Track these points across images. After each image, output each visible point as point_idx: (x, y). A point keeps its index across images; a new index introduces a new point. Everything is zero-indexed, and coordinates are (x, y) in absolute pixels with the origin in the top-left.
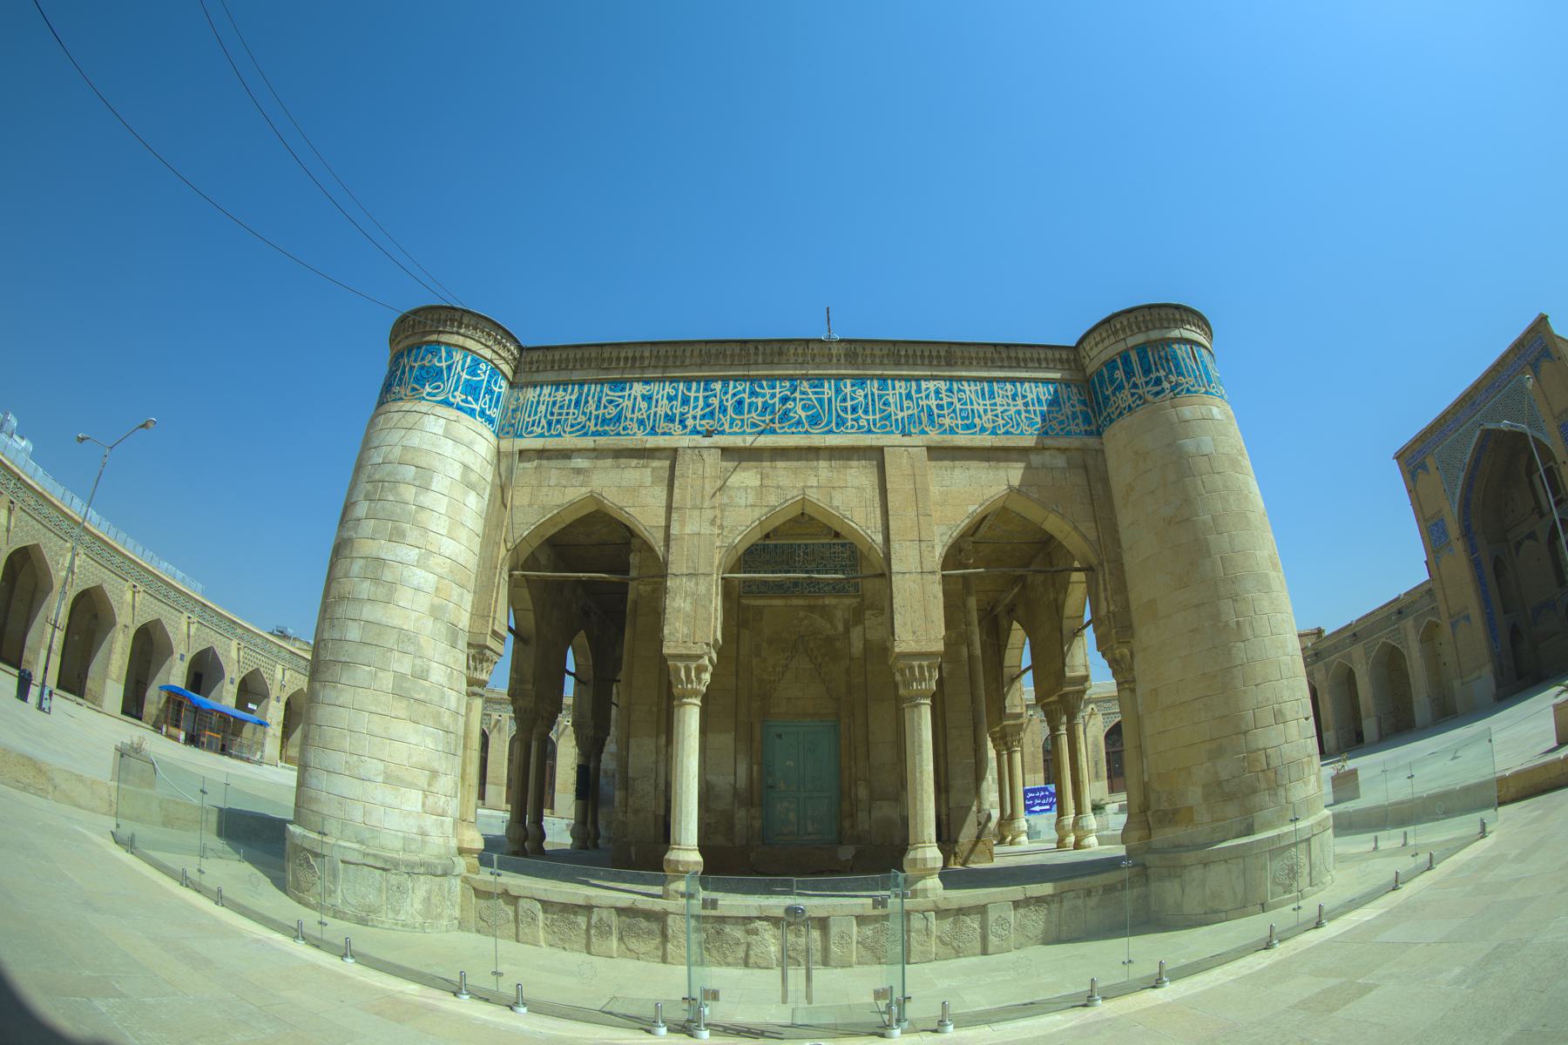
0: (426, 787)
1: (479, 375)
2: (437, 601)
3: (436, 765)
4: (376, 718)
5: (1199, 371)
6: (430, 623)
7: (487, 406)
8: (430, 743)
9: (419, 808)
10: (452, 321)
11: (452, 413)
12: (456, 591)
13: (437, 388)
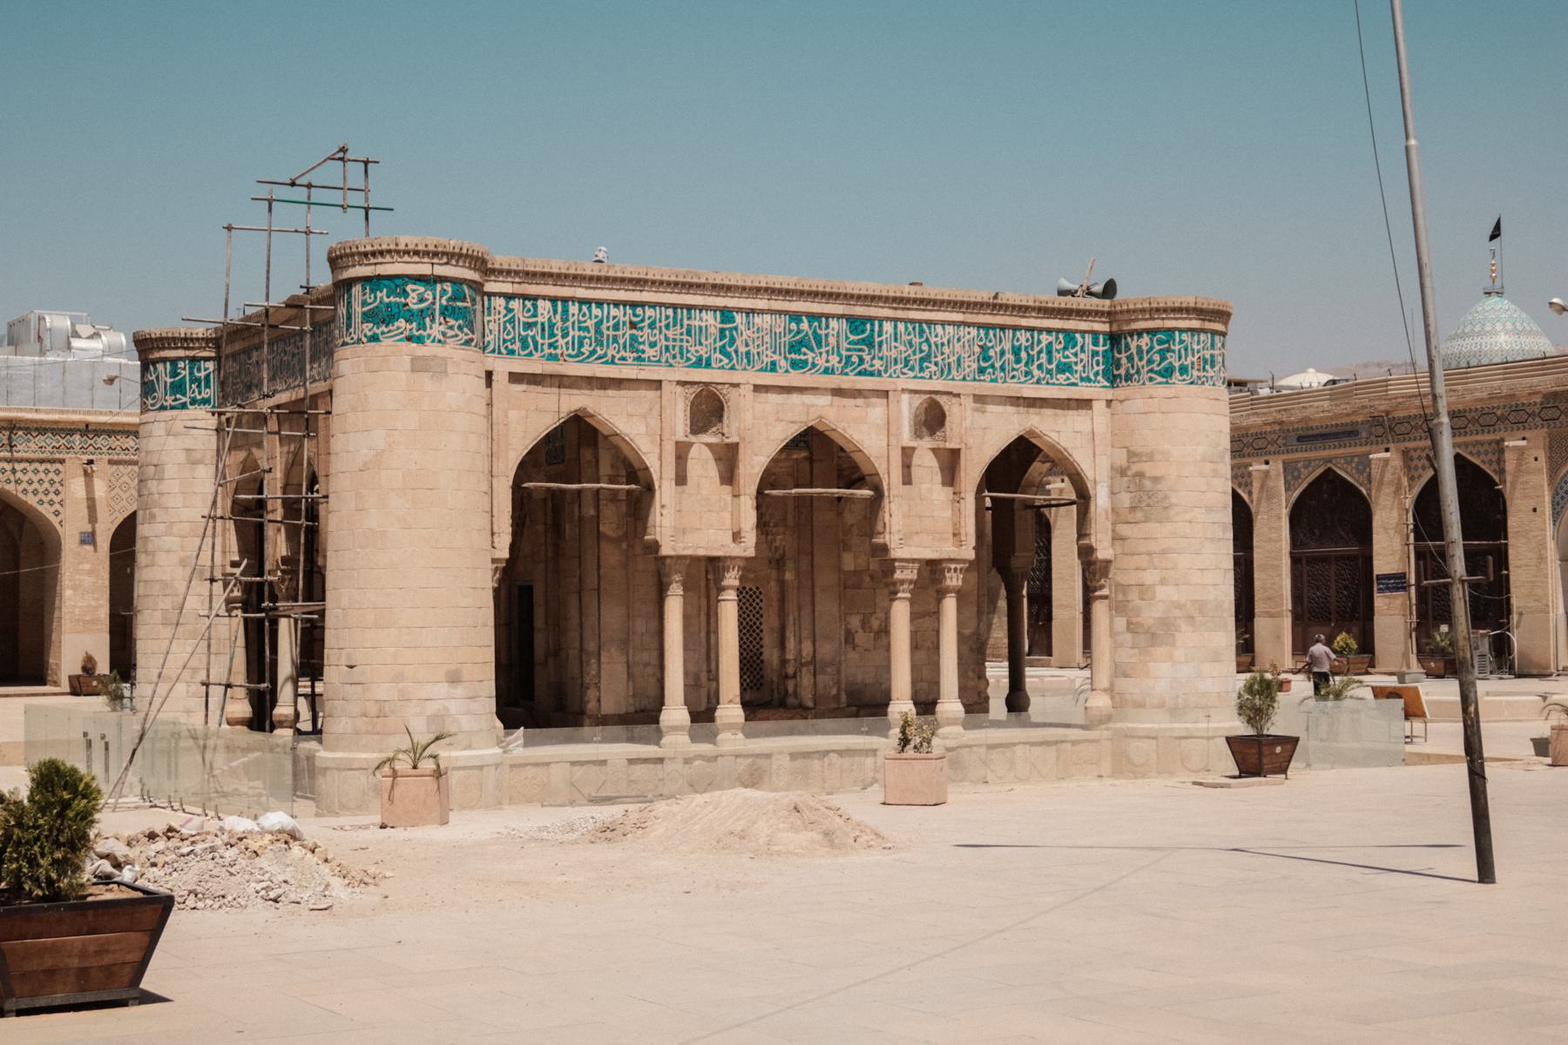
1: (180, 374)
7: (197, 393)
9: (185, 694)
13: (154, 398)
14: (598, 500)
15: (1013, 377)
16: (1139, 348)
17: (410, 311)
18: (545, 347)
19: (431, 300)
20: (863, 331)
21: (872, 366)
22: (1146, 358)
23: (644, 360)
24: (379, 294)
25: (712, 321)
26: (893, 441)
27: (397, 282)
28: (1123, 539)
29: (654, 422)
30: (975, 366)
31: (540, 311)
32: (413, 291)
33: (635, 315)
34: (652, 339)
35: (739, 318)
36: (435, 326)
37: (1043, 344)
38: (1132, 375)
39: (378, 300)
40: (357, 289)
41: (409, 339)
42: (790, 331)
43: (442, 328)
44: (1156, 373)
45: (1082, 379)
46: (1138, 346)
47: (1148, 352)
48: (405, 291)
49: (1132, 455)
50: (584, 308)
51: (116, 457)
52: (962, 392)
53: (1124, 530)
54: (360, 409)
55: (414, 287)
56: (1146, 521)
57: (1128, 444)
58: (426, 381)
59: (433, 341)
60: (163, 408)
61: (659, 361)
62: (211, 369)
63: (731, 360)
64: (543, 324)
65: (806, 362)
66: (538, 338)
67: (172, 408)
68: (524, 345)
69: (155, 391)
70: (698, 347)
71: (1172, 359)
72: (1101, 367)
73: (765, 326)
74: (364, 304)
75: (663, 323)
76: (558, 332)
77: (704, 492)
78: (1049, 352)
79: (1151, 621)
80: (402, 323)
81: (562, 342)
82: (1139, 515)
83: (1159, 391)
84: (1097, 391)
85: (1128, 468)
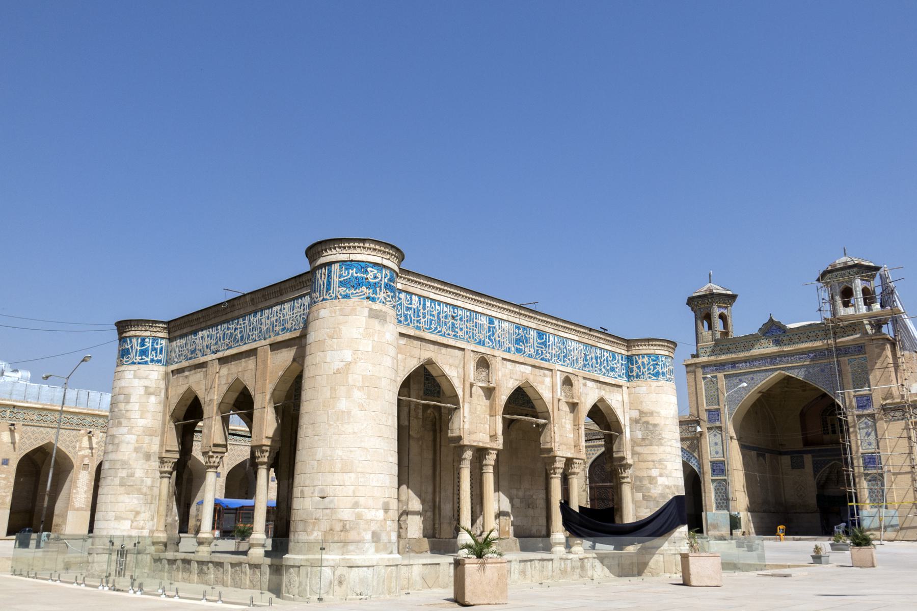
0: (133, 518)
2: (137, 445)
3: (138, 509)
4: (112, 496)
5: (324, 286)
6: (134, 455)
8: (135, 501)
9: (129, 527)
10: (128, 326)
11: (136, 367)
12: (147, 439)
13: (128, 358)
14: (409, 416)
15: (596, 371)
16: (643, 364)
17: (369, 282)
18: (415, 322)
19: (380, 278)
20: (543, 338)
21: (546, 356)
22: (647, 368)
23: (457, 337)
24: (351, 271)
25: (485, 322)
26: (555, 396)
27: (363, 266)
28: (639, 454)
29: (461, 370)
30: (582, 363)
31: (413, 302)
32: (371, 271)
33: (454, 312)
34: (461, 327)
35: (495, 322)
36: (382, 293)
37: (605, 357)
38: (640, 376)
39: (350, 275)
40: (335, 267)
41: (368, 298)
42: (516, 333)
43: (385, 295)
44: (652, 374)
45: (620, 376)
46: (642, 362)
47: (647, 365)
48: (367, 271)
49: (641, 413)
50: (433, 304)
51: (26, 423)
52: (579, 375)
53: (638, 449)
54: (335, 337)
55: (372, 269)
56: (651, 445)
57: (639, 408)
58: (375, 323)
59: (380, 302)
60: (134, 363)
61: (463, 338)
62: (164, 344)
63: (492, 342)
64: (414, 309)
65: (522, 350)
66: (412, 316)
67: (139, 363)
68: (406, 316)
69: (130, 354)
70: (479, 334)
71: (659, 368)
72: (624, 371)
73: (506, 329)
74: (341, 276)
75: (466, 319)
76: (421, 315)
77: (478, 413)
78: (607, 361)
79: (656, 495)
80: (364, 289)
81: (422, 320)
82: (647, 442)
83: (654, 383)
84: (622, 381)
85: (640, 419)
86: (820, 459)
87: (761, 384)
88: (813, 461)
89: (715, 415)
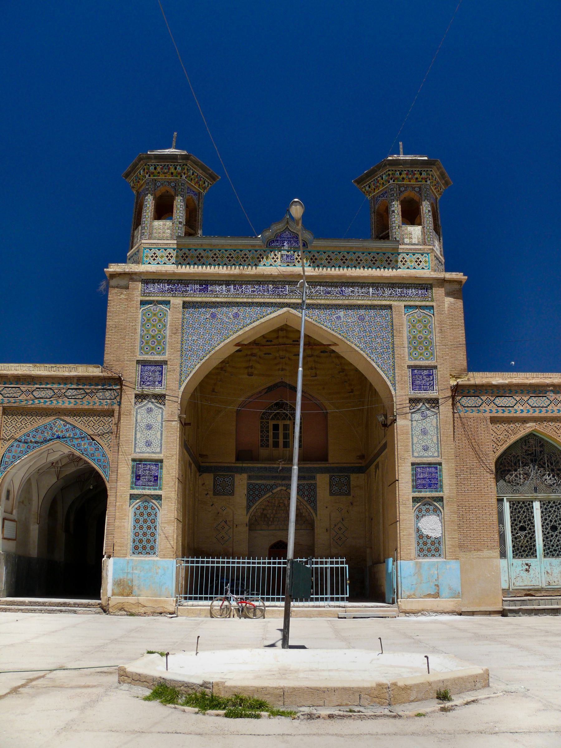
86: (259, 482)
87: (250, 326)
88: (249, 485)
89: (154, 372)
